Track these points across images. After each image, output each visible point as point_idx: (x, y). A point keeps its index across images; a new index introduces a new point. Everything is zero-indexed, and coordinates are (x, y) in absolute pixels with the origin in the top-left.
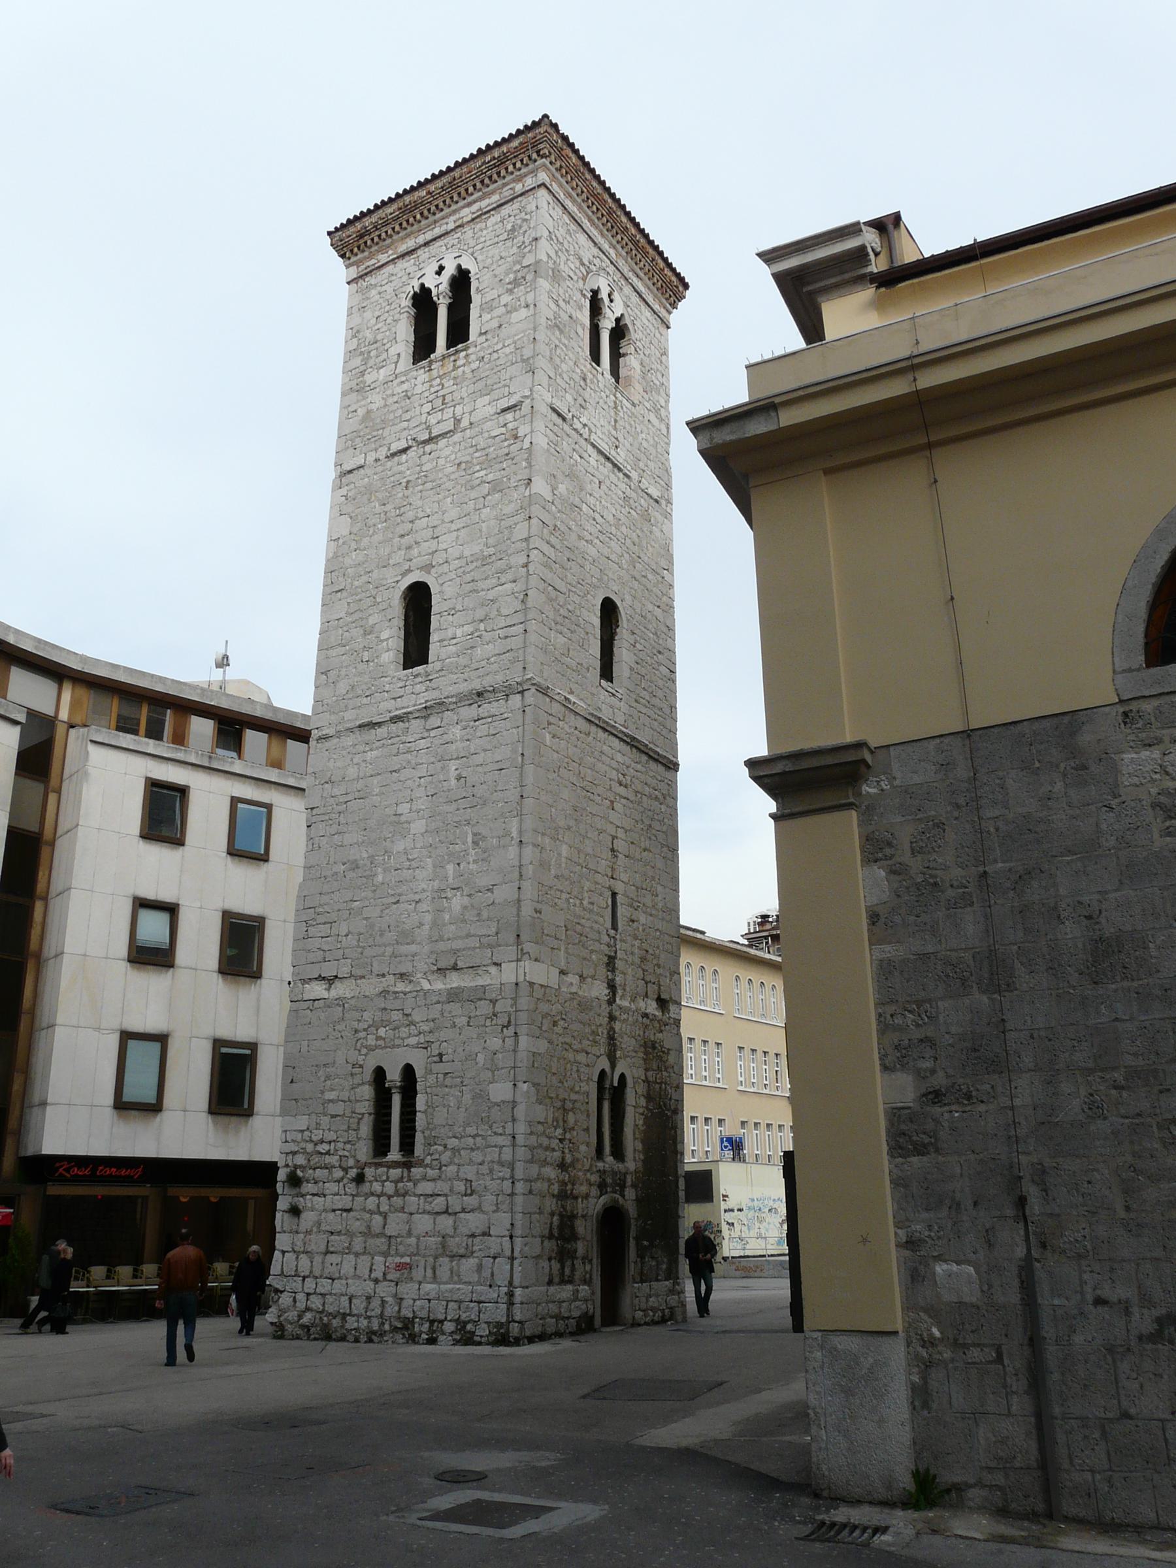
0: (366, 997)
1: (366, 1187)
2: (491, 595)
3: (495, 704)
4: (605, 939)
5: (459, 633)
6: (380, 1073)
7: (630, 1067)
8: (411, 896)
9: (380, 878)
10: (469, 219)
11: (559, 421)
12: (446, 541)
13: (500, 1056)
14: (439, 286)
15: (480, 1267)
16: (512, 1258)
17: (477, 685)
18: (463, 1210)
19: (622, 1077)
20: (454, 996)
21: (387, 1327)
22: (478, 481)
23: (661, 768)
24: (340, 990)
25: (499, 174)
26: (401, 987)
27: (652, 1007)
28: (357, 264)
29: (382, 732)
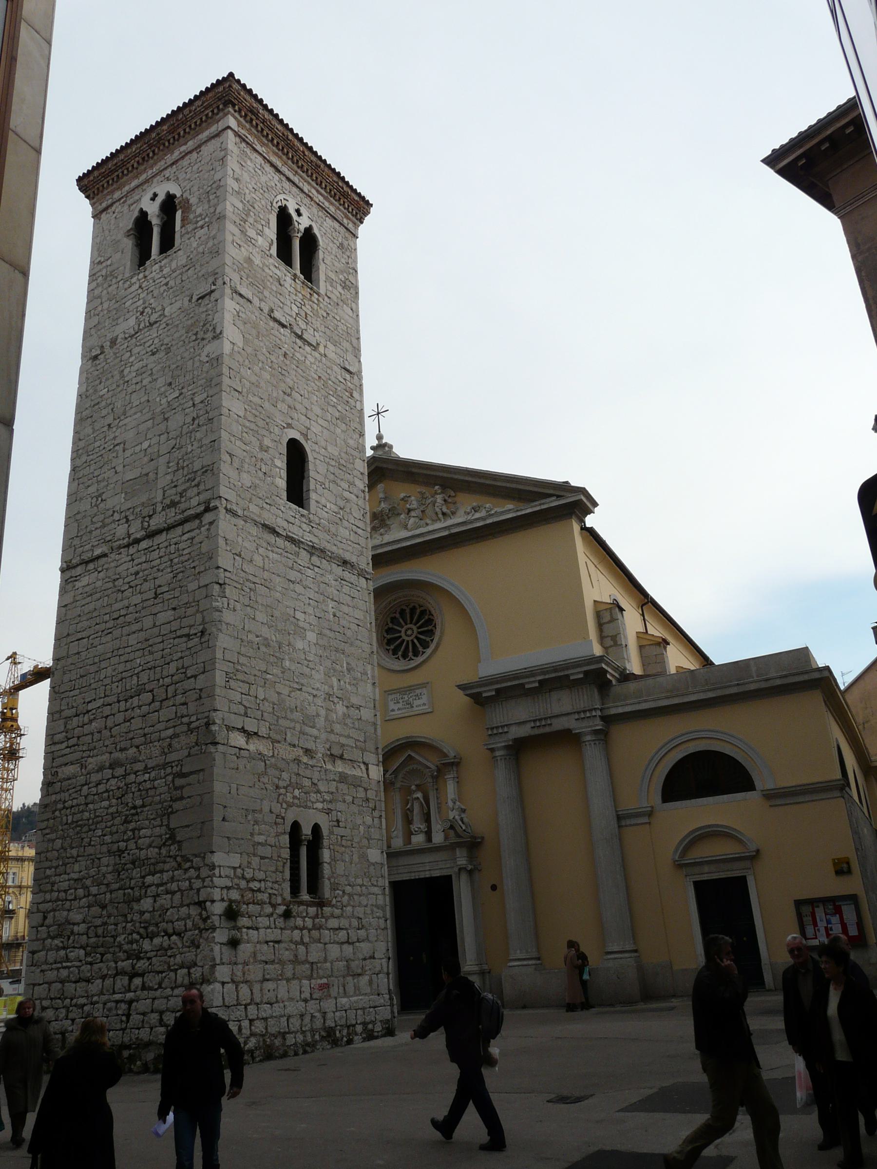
0: (283, 759)
1: (291, 922)
6: (296, 827)
8: (310, 690)
15: (371, 982)
16: (388, 974)
17: (347, 556)
18: (358, 941)
20: (343, 778)
21: (317, 1037)
22: (332, 403)
24: (254, 746)
28: (239, 124)
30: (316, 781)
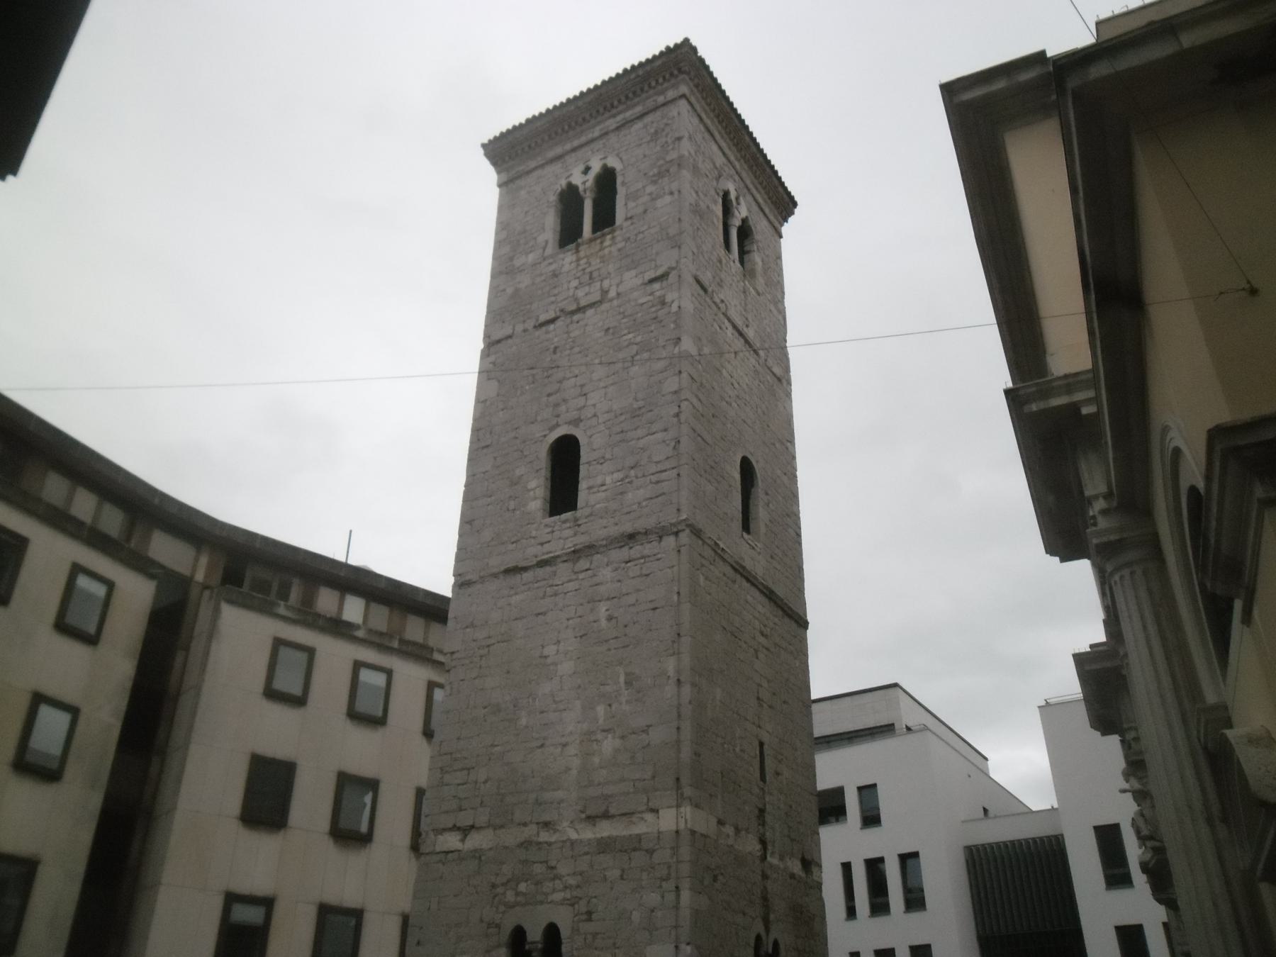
0: (506, 848)
2: (642, 443)
3: (649, 546)
4: (756, 790)
5: (608, 480)
6: (519, 934)
7: (781, 933)
9: (524, 721)
10: (614, 126)
11: (702, 292)
12: (594, 398)
13: (659, 914)
14: (584, 181)
17: (628, 528)
19: (776, 944)
20: (605, 846)
23: (794, 625)
24: (476, 841)
25: (642, 90)
26: (544, 836)
27: (796, 867)
29: (527, 576)
30: (553, 863)
